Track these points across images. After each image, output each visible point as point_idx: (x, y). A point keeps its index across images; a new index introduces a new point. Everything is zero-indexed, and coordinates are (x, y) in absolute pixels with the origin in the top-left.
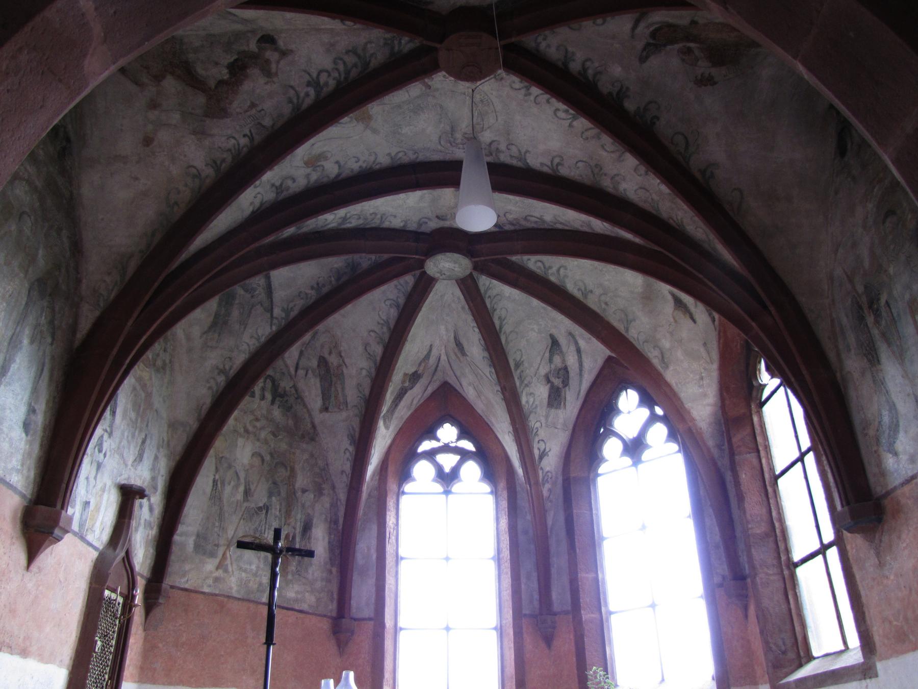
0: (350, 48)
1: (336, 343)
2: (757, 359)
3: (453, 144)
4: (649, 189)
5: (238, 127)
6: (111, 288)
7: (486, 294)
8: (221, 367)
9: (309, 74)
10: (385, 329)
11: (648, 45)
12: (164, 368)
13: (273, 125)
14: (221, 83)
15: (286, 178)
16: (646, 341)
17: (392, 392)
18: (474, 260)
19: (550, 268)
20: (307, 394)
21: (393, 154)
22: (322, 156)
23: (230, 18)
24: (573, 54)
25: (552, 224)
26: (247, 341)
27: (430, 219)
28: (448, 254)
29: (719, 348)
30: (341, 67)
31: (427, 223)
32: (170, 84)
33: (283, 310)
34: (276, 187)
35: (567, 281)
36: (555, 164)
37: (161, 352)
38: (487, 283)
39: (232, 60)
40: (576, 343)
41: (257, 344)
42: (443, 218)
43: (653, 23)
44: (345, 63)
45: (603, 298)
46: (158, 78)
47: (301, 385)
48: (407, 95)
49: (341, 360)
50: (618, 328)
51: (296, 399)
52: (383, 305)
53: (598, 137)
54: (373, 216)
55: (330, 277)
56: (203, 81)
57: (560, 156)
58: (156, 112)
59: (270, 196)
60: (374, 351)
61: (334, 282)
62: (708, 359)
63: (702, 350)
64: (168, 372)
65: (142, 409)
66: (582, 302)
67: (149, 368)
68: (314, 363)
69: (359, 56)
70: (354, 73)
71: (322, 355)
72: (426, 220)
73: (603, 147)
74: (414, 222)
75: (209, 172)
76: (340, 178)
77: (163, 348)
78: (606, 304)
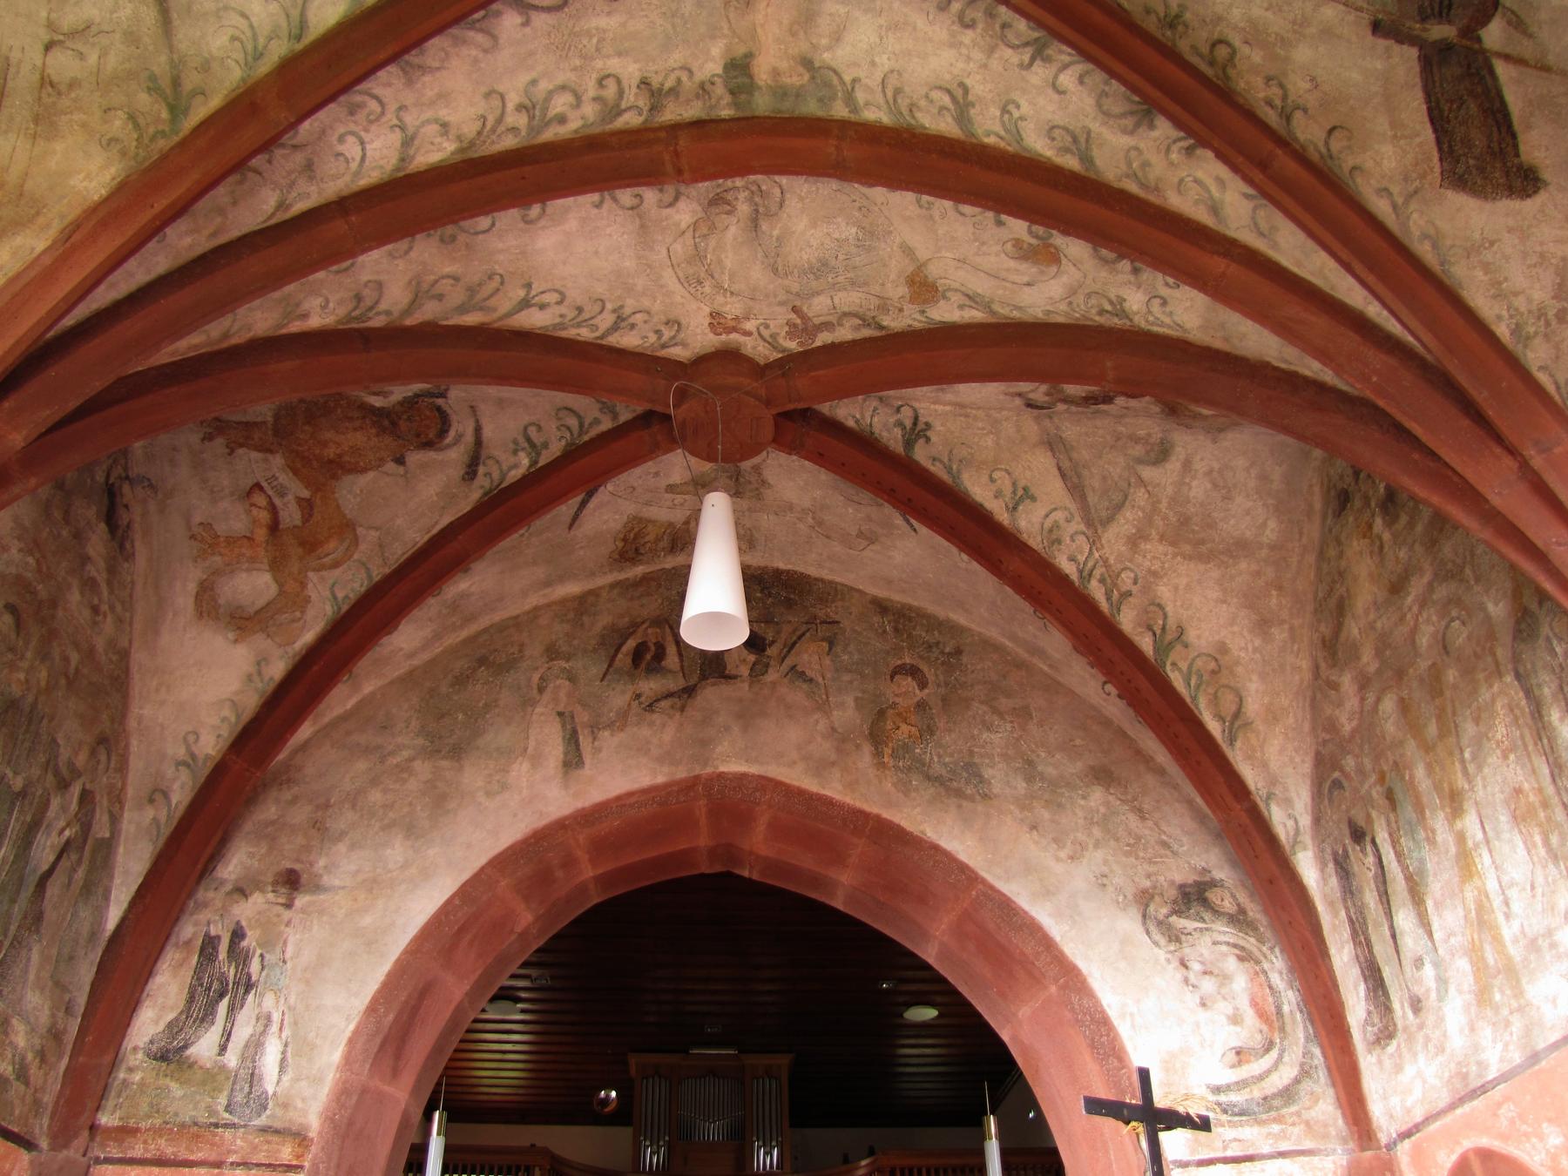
3: (754, 188)
48: (836, 300)
54: (971, 14)
57: (530, 222)
73: (456, 279)
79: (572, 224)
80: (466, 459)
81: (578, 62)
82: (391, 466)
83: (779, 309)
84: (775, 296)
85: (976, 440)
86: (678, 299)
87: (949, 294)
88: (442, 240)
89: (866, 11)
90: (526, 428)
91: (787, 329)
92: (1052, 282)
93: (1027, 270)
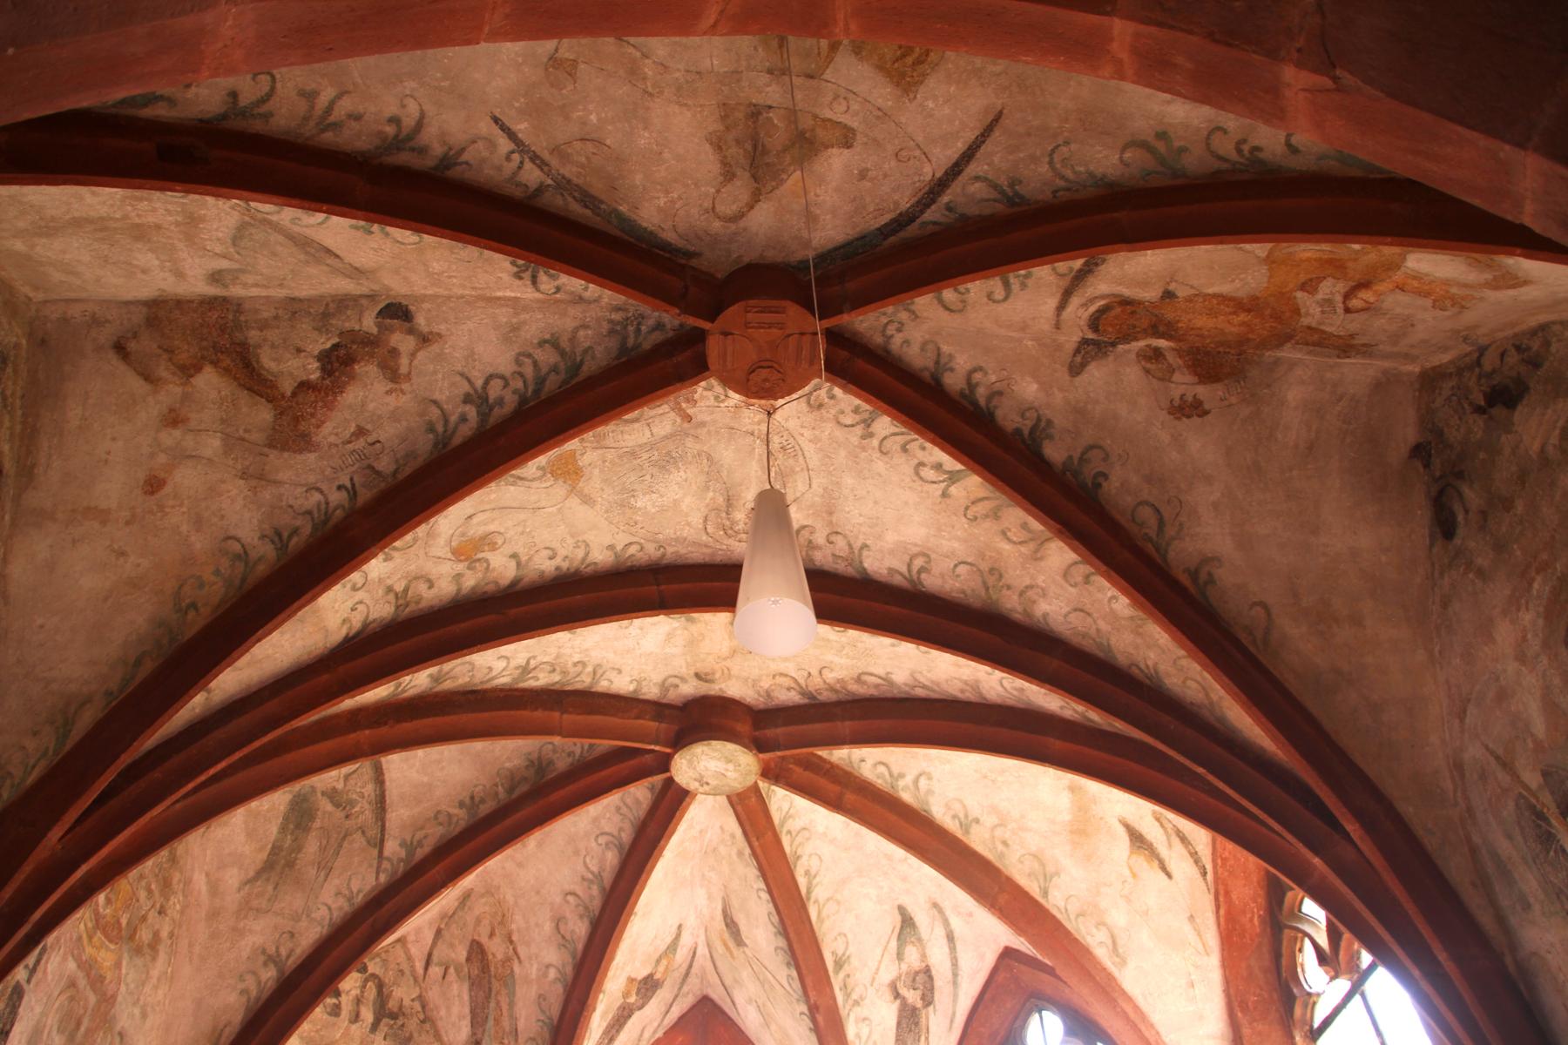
0: (547, 337)
1: (504, 916)
2: (1295, 943)
3: (730, 532)
4: (1090, 611)
5: (328, 471)
6: (32, 762)
7: (782, 826)
8: (272, 950)
9: (469, 381)
10: (595, 890)
11: (1085, 342)
12: (154, 945)
13: (396, 472)
14: (304, 386)
15: (417, 578)
16: (1080, 914)
17: (605, 1013)
18: (761, 756)
19: (902, 776)
20: (443, 1013)
21: (619, 548)
22: (487, 542)
23: (329, 261)
24: (951, 356)
25: (907, 689)
26: (330, 902)
27: (683, 679)
28: (714, 743)
29: (1219, 925)
30: (529, 371)
31: (677, 686)
32: (209, 382)
33: (403, 844)
34: (396, 594)
35: (932, 800)
36: (915, 569)
37: (153, 914)
38: (786, 807)
39: (328, 345)
40: (946, 923)
41: (347, 908)
42: (708, 677)
43: (1096, 297)
44: (535, 363)
45: (999, 832)
46: (188, 371)
47: (433, 995)
48: (648, 434)
49: (511, 948)
50: (1027, 889)
51: (423, 1022)
52: (594, 844)
53: (995, 515)
54: (579, 668)
55: (496, 785)
56: (271, 381)
58: (177, 433)
59: (382, 610)
60: (573, 931)
61: (502, 794)
62: (1200, 947)
63: (1187, 928)
64: (162, 956)
65: (83, 1029)
66: (961, 841)
67: (117, 944)
68: (461, 954)
69: (562, 353)
70: (552, 384)
71: (476, 938)
72: (676, 681)
73: (1004, 533)
74: (654, 684)
75: (268, 551)
76: (519, 587)
77: (158, 906)
78: (1005, 843)
79: (891, 538)
80: (1091, 279)
81: (859, 645)
82: (1182, 293)
83: (707, 418)
84: (709, 432)
85: (454, 267)
86: (807, 433)
87: (540, 473)
88: (1001, 576)
89: (651, 653)
90: (1006, 298)
91: (696, 396)
92: (451, 532)
93: (477, 529)
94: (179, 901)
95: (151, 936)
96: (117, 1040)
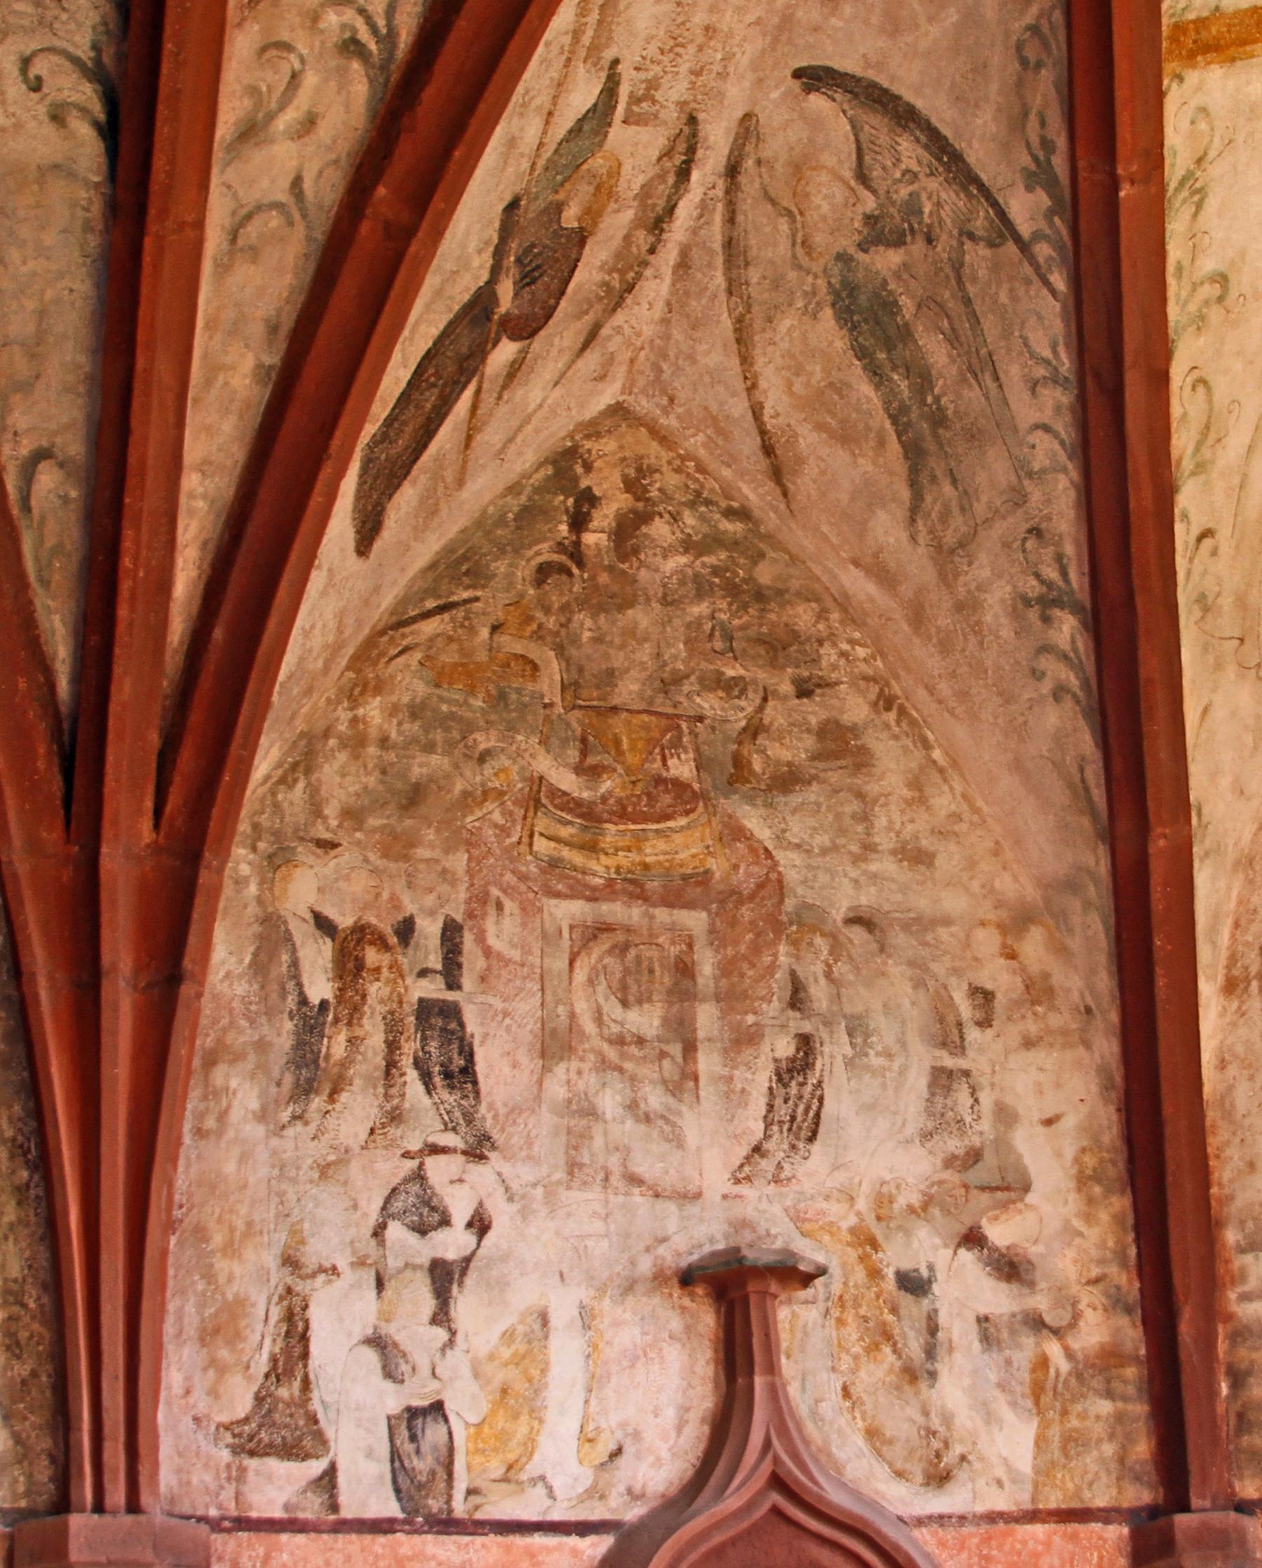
94: (852, 642)
95: (810, 742)
96: (858, 934)
